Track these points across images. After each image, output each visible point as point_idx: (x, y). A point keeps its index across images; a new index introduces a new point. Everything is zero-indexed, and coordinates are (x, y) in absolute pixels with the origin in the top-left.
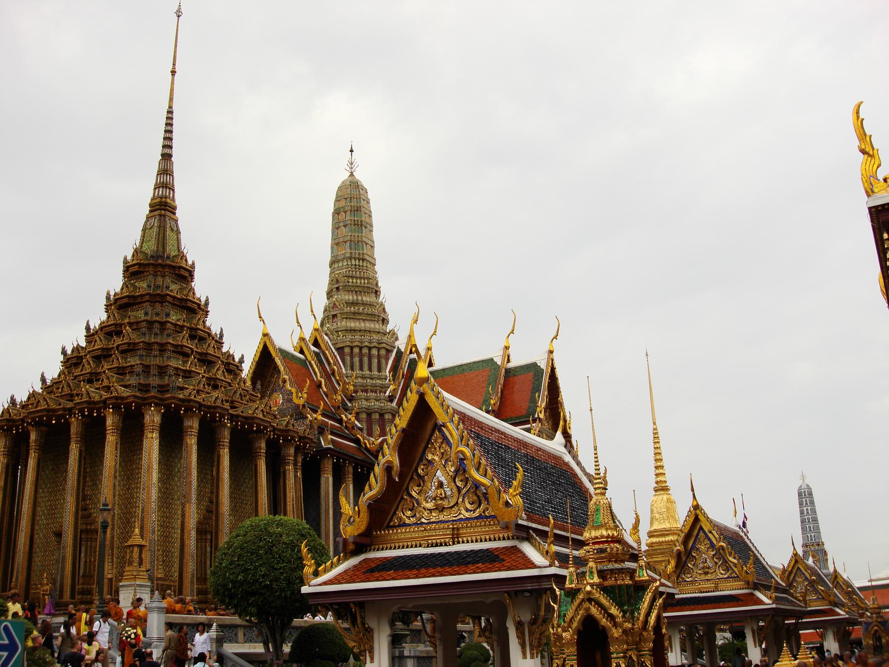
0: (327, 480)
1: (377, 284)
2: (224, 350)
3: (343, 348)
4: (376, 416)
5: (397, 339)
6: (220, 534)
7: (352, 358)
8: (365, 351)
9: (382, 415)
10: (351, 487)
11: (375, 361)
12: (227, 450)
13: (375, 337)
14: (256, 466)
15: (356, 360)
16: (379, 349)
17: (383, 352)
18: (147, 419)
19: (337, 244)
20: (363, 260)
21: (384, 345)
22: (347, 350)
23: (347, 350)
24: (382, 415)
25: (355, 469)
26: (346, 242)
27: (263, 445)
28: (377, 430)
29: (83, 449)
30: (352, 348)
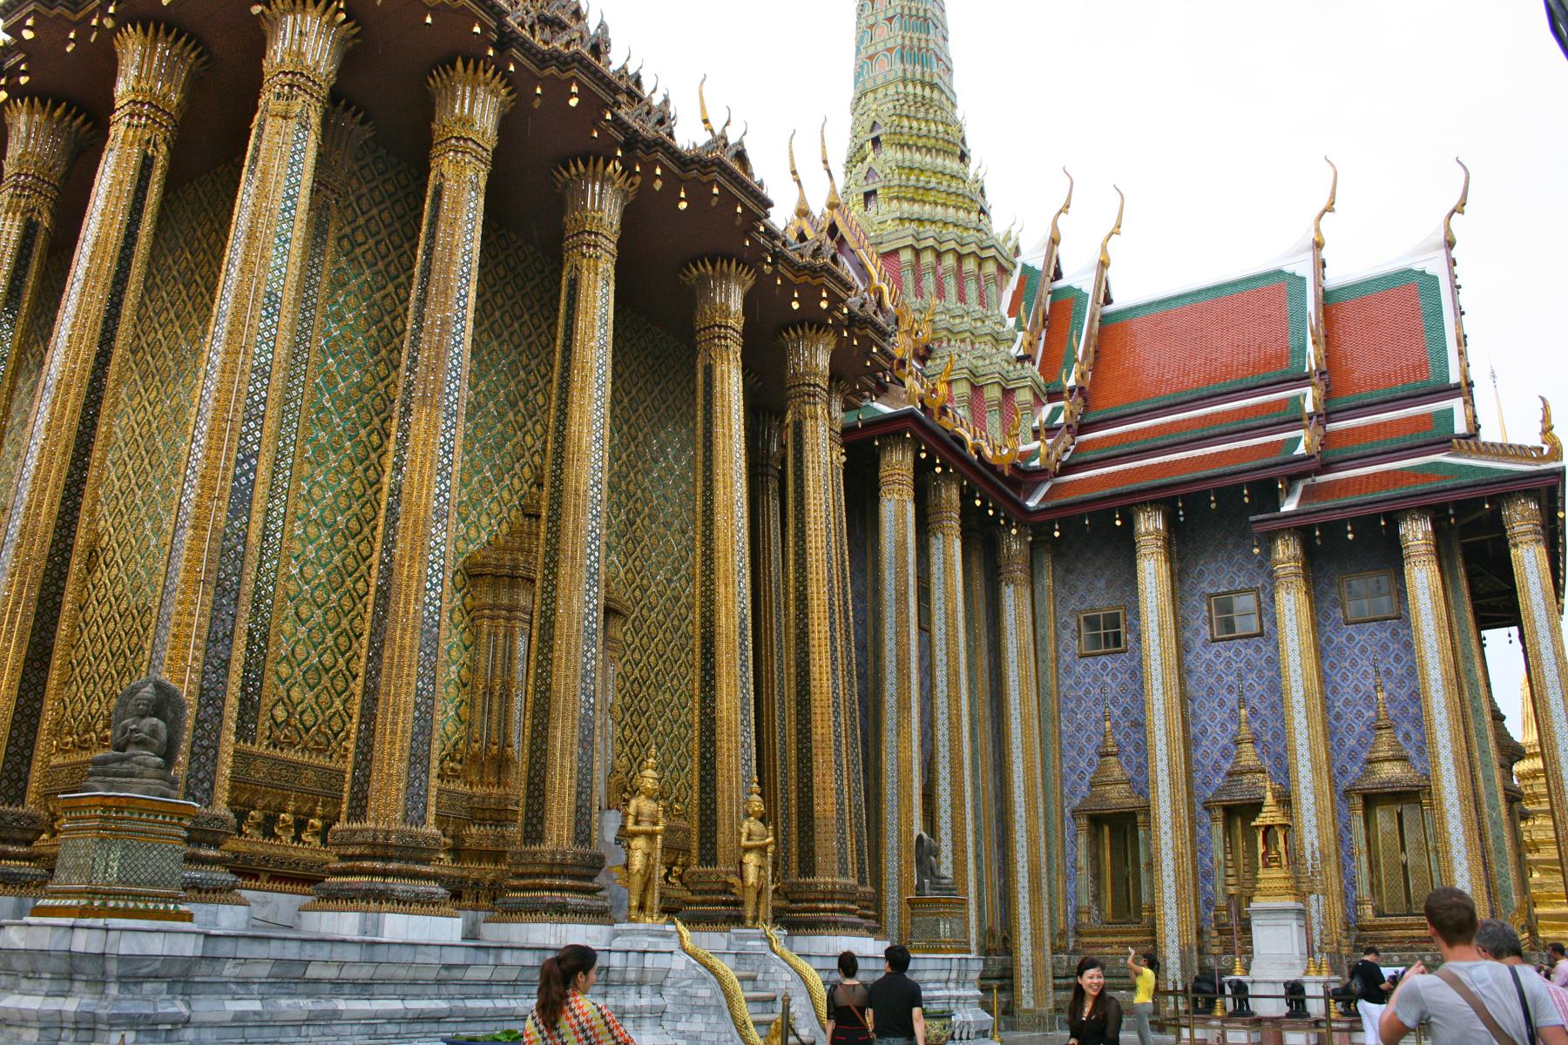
0: (896, 509)
1: (963, 141)
2: (614, 67)
3: (895, 252)
4: (993, 393)
5: (1017, 251)
6: (564, 570)
7: (918, 280)
8: (949, 261)
9: (1008, 393)
10: (958, 544)
11: (972, 290)
12: (607, 266)
13: (970, 236)
14: (709, 371)
15: (929, 283)
16: (981, 262)
17: (990, 268)
18: (278, 52)
19: (871, 58)
20: (933, 86)
21: (992, 252)
22: (906, 256)
23: (906, 256)
24: (1008, 393)
25: (966, 497)
26: (890, 50)
27: (736, 303)
28: (994, 422)
29: (45, 221)
30: (917, 253)
